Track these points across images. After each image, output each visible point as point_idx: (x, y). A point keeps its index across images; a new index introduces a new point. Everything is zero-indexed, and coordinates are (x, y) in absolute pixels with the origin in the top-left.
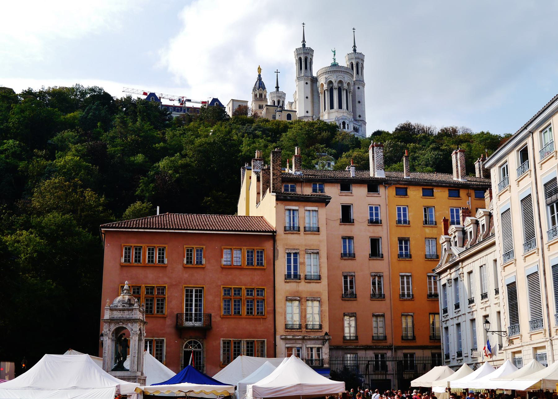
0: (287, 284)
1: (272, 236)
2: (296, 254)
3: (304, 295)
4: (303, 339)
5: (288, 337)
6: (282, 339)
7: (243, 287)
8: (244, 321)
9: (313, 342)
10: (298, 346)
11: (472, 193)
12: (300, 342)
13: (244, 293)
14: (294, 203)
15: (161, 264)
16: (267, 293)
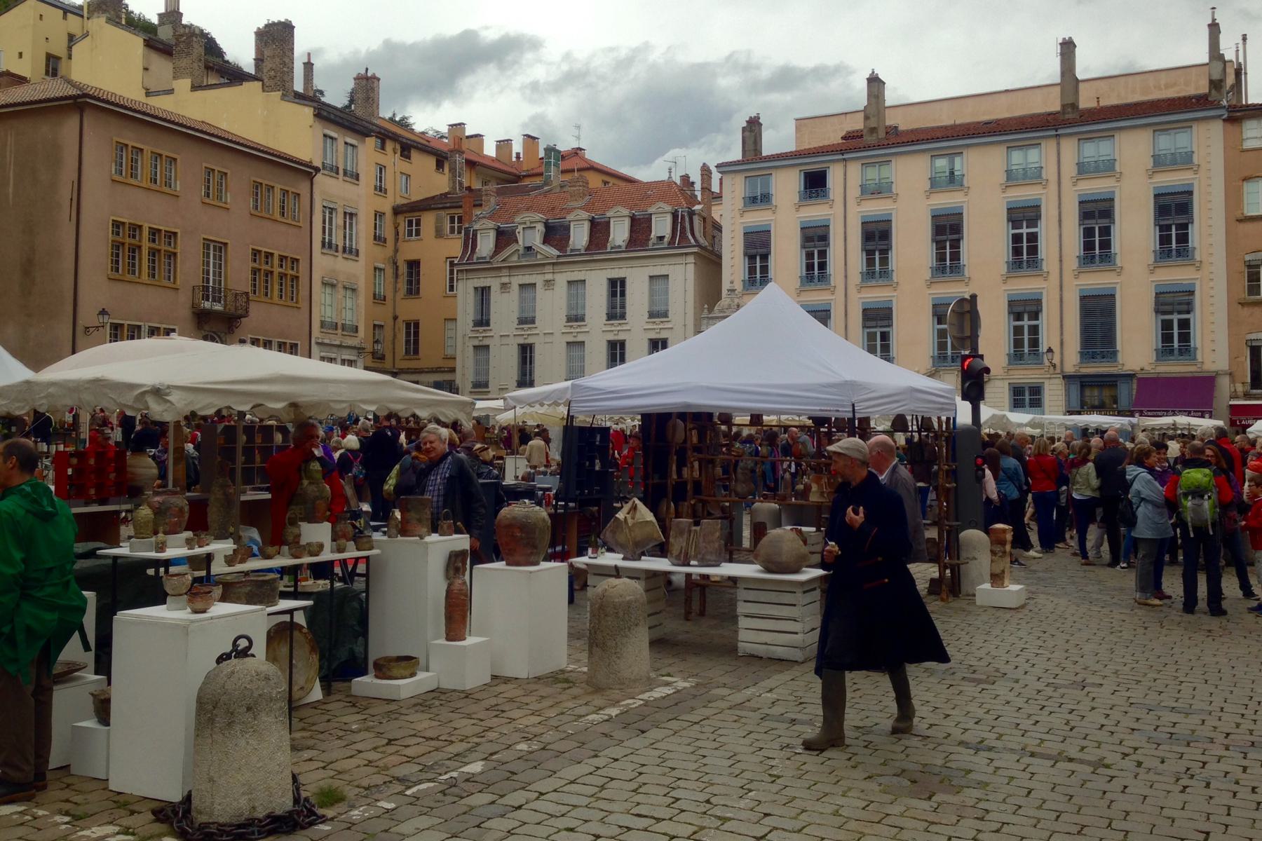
0: (325, 257)
1: (306, 172)
2: (332, 210)
3: (341, 278)
4: (340, 346)
5: (327, 341)
6: (317, 343)
7: (276, 253)
8: (277, 308)
9: (348, 351)
10: (333, 356)
11: (398, 147)
12: (335, 350)
13: (276, 261)
14: (333, 127)
15: (167, 189)
16: (303, 266)
